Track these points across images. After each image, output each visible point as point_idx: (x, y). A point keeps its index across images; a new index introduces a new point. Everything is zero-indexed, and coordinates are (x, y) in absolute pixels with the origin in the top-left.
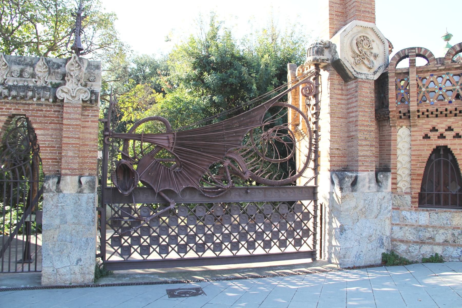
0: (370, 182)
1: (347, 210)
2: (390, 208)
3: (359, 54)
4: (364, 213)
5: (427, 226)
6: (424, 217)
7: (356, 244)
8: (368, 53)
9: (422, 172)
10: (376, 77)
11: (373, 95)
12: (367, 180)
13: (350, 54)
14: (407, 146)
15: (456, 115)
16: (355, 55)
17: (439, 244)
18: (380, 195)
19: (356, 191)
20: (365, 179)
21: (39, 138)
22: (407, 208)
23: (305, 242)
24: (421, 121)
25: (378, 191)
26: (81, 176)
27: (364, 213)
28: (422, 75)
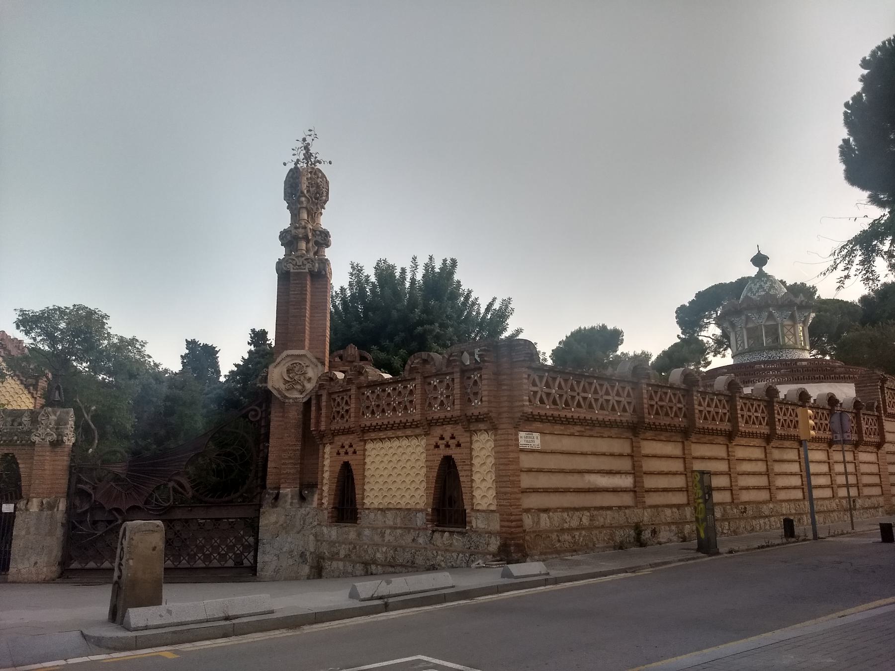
0: (292, 498)
1: (266, 525)
2: (316, 523)
3: (288, 379)
4: (284, 528)
5: (335, 543)
6: (332, 533)
7: (275, 558)
8: (302, 378)
9: (334, 487)
10: (305, 400)
11: (300, 416)
12: (290, 496)
13: (282, 381)
14: (328, 461)
15: (353, 433)
16: (286, 382)
17: (341, 560)
18: (303, 511)
19: (276, 507)
20: (287, 495)
21: (21, 470)
22: (325, 523)
23: (246, 557)
24: (336, 438)
25: (301, 507)
26: (44, 498)
27: (286, 528)
28: (333, 396)
